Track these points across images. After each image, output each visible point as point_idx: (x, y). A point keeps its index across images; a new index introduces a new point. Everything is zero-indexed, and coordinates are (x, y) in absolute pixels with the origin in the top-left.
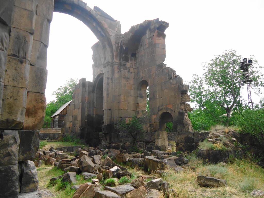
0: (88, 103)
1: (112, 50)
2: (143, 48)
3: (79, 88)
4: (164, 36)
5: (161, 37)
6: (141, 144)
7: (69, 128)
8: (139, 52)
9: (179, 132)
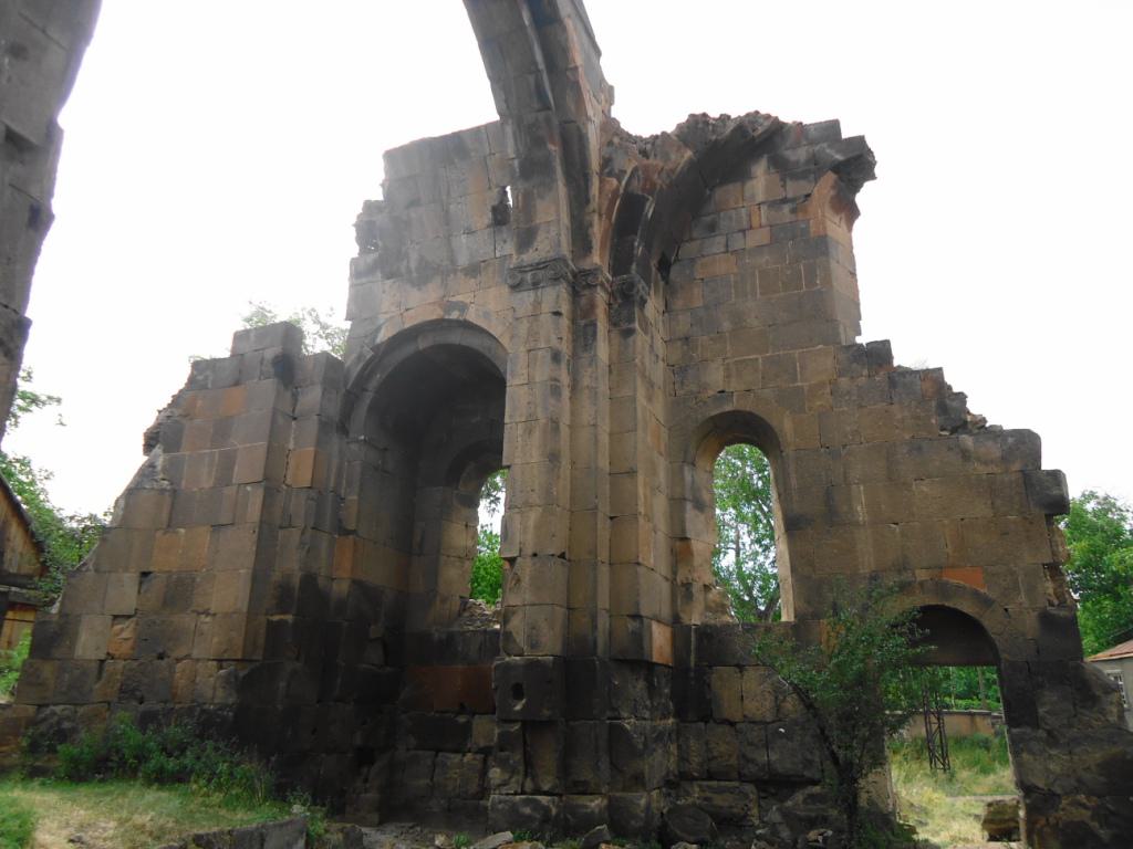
0: (313, 494)
1: (579, 199)
2: (727, 246)
3: (237, 383)
4: (852, 213)
5: (843, 215)
6: (720, 791)
7: (95, 665)
8: (693, 260)
9: (1049, 733)
